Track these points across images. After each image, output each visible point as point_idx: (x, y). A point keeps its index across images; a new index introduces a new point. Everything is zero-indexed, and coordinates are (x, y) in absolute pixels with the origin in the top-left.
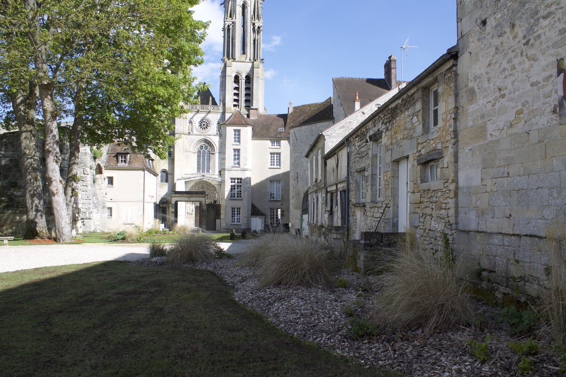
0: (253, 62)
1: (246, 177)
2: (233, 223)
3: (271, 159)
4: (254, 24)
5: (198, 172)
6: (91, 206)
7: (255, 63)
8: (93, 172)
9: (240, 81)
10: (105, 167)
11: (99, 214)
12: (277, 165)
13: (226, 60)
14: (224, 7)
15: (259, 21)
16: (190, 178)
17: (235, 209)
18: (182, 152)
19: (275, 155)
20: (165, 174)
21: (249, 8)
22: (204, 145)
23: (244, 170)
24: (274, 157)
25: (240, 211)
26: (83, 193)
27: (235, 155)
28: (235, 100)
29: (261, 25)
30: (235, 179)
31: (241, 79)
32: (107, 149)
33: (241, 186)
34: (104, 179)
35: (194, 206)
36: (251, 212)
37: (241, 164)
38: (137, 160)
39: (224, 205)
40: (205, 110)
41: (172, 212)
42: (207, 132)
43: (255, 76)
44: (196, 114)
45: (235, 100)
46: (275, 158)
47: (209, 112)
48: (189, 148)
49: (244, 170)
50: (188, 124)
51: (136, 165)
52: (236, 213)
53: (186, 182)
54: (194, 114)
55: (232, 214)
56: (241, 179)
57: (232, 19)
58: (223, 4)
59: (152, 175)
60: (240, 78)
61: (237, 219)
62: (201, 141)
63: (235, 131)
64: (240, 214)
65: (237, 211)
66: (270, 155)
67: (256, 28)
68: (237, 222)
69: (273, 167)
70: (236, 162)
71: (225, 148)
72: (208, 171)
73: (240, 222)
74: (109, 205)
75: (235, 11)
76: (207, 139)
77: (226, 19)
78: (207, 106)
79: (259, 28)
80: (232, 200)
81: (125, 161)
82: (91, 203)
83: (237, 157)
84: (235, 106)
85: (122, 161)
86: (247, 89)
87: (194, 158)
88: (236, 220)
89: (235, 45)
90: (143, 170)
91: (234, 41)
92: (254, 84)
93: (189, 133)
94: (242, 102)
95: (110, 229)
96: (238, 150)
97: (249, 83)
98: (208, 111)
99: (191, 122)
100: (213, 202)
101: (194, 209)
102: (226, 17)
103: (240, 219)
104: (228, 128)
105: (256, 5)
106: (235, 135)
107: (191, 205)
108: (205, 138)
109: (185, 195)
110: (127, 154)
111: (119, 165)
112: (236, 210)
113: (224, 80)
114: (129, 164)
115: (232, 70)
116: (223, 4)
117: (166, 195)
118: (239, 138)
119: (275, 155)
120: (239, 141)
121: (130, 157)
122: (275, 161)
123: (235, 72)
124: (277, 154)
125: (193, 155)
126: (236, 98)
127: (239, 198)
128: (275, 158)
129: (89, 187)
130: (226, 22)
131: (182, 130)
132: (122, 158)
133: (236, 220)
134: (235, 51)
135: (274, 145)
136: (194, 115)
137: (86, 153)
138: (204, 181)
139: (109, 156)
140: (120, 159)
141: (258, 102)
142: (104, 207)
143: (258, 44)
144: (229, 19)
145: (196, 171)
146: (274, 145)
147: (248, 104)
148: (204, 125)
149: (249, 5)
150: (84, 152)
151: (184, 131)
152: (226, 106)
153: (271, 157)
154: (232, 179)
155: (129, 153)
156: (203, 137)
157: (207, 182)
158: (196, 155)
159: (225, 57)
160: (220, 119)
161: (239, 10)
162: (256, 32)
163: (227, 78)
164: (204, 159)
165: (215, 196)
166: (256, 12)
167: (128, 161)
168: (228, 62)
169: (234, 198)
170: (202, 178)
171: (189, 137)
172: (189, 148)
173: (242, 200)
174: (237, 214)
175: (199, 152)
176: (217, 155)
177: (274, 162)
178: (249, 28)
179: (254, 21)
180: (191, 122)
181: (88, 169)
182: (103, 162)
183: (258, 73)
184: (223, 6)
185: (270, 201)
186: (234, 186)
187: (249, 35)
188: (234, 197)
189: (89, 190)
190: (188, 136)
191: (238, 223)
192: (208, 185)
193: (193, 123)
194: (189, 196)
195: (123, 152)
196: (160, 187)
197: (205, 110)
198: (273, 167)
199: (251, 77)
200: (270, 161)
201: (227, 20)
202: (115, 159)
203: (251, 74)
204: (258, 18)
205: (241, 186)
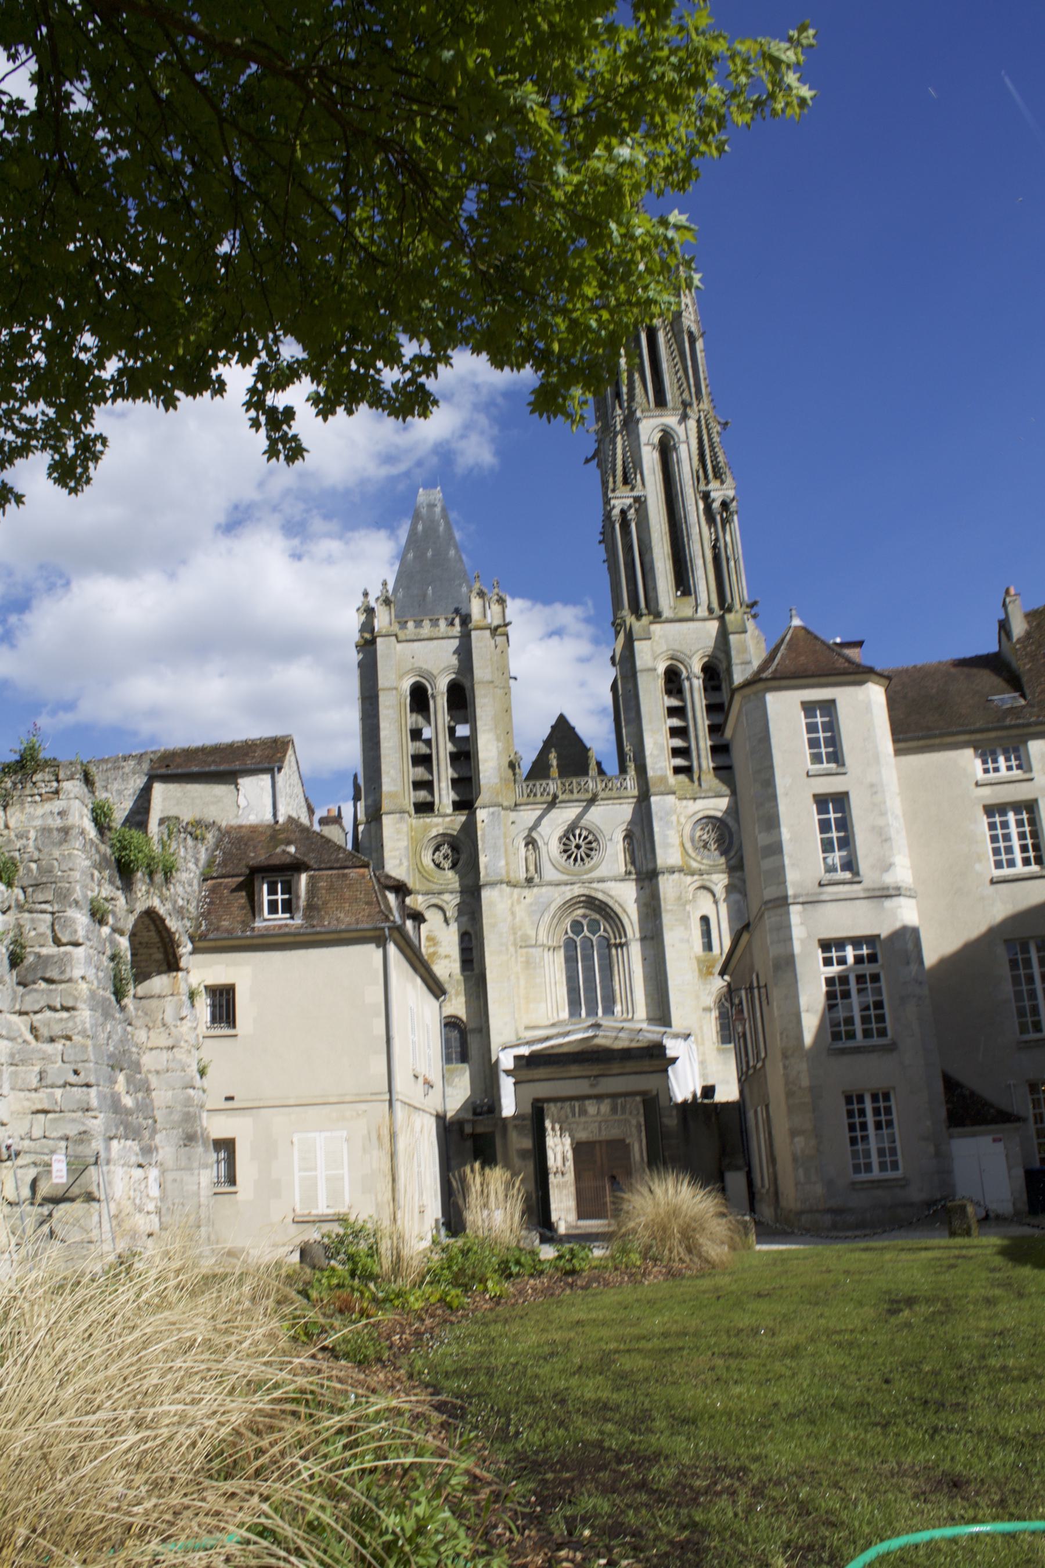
1: (898, 925)
2: (863, 1176)
3: (994, 839)
4: (706, 496)
6: (97, 1124)
7: (729, 617)
8: (113, 943)
9: (686, 684)
10: (192, 939)
11: (154, 1173)
12: (1026, 862)
13: (630, 619)
14: (599, 465)
15: (722, 482)
16: (548, 1038)
17: (861, 1099)
18: (512, 949)
19: (1011, 817)
20: (455, 1034)
21: (683, 449)
22: (584, 916)
23: (884, 894)
24: (1005, 825)
25: (888, 1111)
26: (49, 1048)
27: (824, 826)
28: (676, 752)
29: (731, 493)
30: (840, 944)
31: (688, 678)
32: (203, 856)
33: (875, 978)
34: (192, 995)
35: (568, 1141)
36: (943, 1113)
37: (863, 865)
38: (347, 894)
39: (805, 1082)
40: (576, 796)
41: (523, 1154)
42: (591, 870)
44: (546, 811)
45: (676, 752)
46: (1014, 830)
47: (592, 801)
48: (532, 933)
49: (884, 894)
50: (523, 850)
51: (343, 918)
52: (870, 1119)
54: (538, 813)
55: (852, 1128)
56: (871, 940)
57: (632, 489)
58: (593, 457)
59: (419, 981)
60: (684, 674)
61: (881, 1152)
62: (571, 904)
63: (809, 708)
64: (890, 1124)
65: (877, 1112)
66: (985, 820)
67: (716, 505)
68: (883, 1167)
69: (1006, 872)
70: (836, 857)
71: (774, 797)
72: (609, 1010)
73: (895, 1166)
74: (218, 1127)
75: (638, 464)
76: (594, 894)
77: (614, 491)
78: (583, 780)
79: (725, 505)
80: (843, 1052)
81: (288, 907)
82: (94, 1103)
83: (834, 834)
84: (677, 770)
85: (273, 907)
87: (554, 966)
88: (875, 1160)
89: (652, 569)
90: (380, 942)
91: (647, 559)
93: (529, 881)
94: (703, 753)
95: (230, 1254)
96: (841, 800)
97: (717, 688)
98: (589, 796)
99: (531, 842)
100: (699, 1093)
101: (570, 1155)
102: (611, 485)
103: (893, 1151)
104: (770, 698)
105: (705, 437)
106: (811, 728)
107: (557, 1140)
108: (586, 892)
109: (575, 1070)
110: (297, 867)
111: (258, 924)
112: (868, 1106)
113: (630, 686)
114: (307, 917)
115: (653, 651)
116: (593, 457)
118: (834, 741)
119: (1011, 817)
120: (836, 757)
121: (312, 883)
122: (1016, 843)
123: (664, 656)
124: (1017, 807)
125: (548, 956)
126: (678, 743)
127: (876, 1041)
128: (1014, 830)
129: (85, 1015)
130: (613, 502)
131: (504, 872)
132: (272, 891)
133: (875, 1160)
134: (655, 588)
135: (996, 770)
136: (540, 818)
137: (65, 831)
139: (213, 890)
140: (266, 898)
142: (190, 1139)
143: (728, 560)
144: (623, 491)
145: (565, 1014)
146: (996, 770)
147: (723, 761)
148: (578, 847)
149: (683, 437)
150: (58, 822)
151: (512, 875)
152: (650, 773)
153: (992, 826)
154: (826, 945)
155: (306, 868)
156: (577, 890)
159: (626, 612)
160: (631, 823)
161: (650, 458)
162: (718, 518)
164: (589, 969)
166: (708, 457)
167: (302, 903)
168: (638, 626)
169: (850, 1044)
170: (590, 1034)
171: (531, 894)
172: (532, 933)
173: (892, 1048)
174: (878, 1126)
175: (570, 946)
176: (636, 949)
177: (1009, 850)
178: (691, 508)
179: (707, 484)
180: (531, 842)
181: (81, 919)
182: (180, 912)
183: (744, 649)
184: (595, 462)
185: (1026, 1045)
186: (843, 979)
187: (695, 531)
188: (851, 1035)
189: (84, 1033)
190: (526, 892)
191: (890, 1174)
193: (540, 843)
194: (595, 1070)
195: (275, 861)
197: (576, 796)
198: (1006, 872)
199: (723, 666)
200: (990, 846)
201: (617, 494)
202: (242, 897)
204: (718, 475)
205: (875, 978)
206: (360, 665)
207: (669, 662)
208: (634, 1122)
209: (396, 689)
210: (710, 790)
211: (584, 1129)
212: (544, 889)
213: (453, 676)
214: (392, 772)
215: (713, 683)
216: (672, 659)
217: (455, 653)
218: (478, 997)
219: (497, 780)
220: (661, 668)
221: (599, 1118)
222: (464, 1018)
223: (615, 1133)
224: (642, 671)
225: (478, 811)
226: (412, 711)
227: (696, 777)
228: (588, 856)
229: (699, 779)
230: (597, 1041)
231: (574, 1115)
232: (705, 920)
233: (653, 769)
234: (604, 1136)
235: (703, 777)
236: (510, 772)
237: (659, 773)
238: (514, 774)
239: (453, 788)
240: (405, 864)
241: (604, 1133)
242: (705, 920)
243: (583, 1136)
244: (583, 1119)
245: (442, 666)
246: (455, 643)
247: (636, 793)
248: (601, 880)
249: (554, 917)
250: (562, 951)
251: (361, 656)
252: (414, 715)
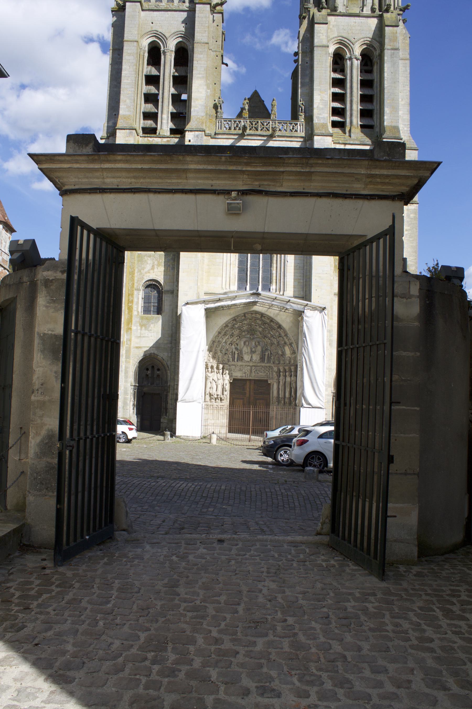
0: (380, 18)
5: (239, 288)
20: (155, 293)
31: (350, 59)
35: (227, 377)
40: (259, 132)
43: (387, 46)
53: (209, 313)
72: (267, 288)
78: (266, 121)
86: (365, 84)
92: (386, 65)
97: (370, 71)
101: (228, 387)
107: (220, 376)
113: (308, 59)
117: (157, 345)
138: (256, 312)
141: (395, 109)
145: (234, 287)
147: (368, 122)
152: (316, 121)
157: (262, 315)
163: (317, 53)
165: (283, 354)
168: (319, 15)
170: (251, 299)
183: (395, 39)
192: (264, 323)
196: (141, 326)
199: (377, 53)
203: (376, 45)
206: (114, 25)
207: (338, 46)
208: (275, 369)
209: (137, 42)
210: (357, 139)
211: (240, 370)
213: (180, 40)
214: (128, 101)
215: (366, 68)
216: (340, 43)
217: (183, 22)
218: (173, 268)
219: (203, 114)
220: (332, 49)
221: (251, 364)
222: (162, 282)
223: (261, 375)
224: (317, 46)
225: (187, 133)
226: (148, 64)
227: (347, 129)
229: (350, 131)
230: (256, 308)
231: (233, 360)
233: (318, 118)
234: (254, 376)
235: (353, 130)
236: (214, 111)
237: (322, 121)
238: (217, 113)
239: (172, 121)
241: (253, 374)
243: (238, 375)
244: (240, 363)
245: (173, 32)
246: (185, 15)
247: (303, 134)
251: (115, 19)
252: (150, 67)
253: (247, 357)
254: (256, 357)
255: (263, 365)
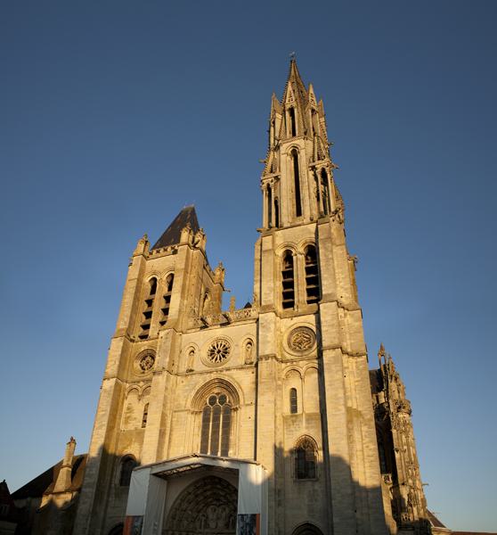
22: (218, 394)
125: (191, 417)
156: (213, 376)
158: (200, 418)
207: (284, 249)
212: (194, 377)
228: (224, 356)
231: (200, 528)
232: (294, 390)
240: (117, 363)
242: (294, 390)
244: (206, 530)
248: (228, 370)
249: (197, 393)
250: (202, 415)
253: (212, 525)
254: (221, 524)
255: (227, 531)
